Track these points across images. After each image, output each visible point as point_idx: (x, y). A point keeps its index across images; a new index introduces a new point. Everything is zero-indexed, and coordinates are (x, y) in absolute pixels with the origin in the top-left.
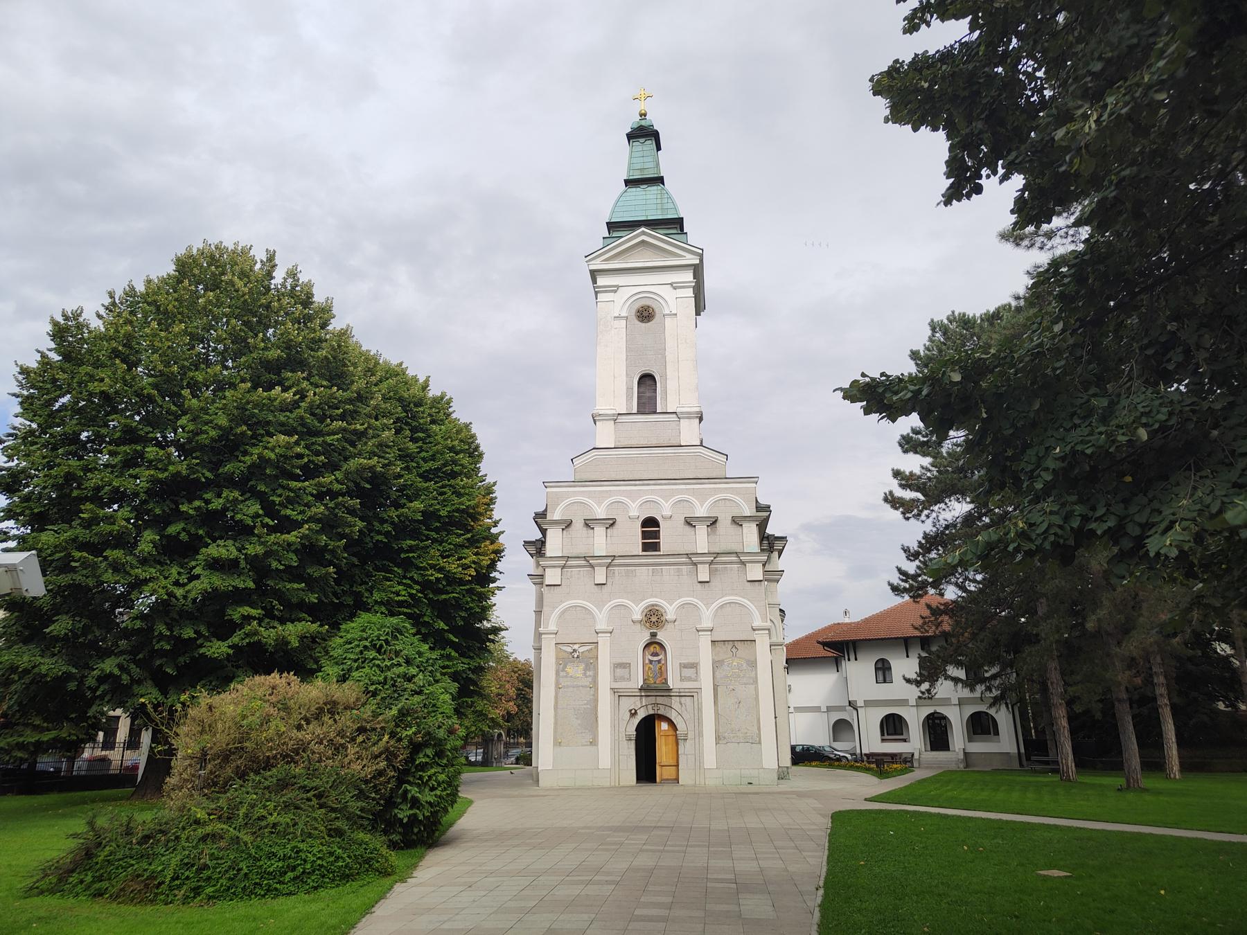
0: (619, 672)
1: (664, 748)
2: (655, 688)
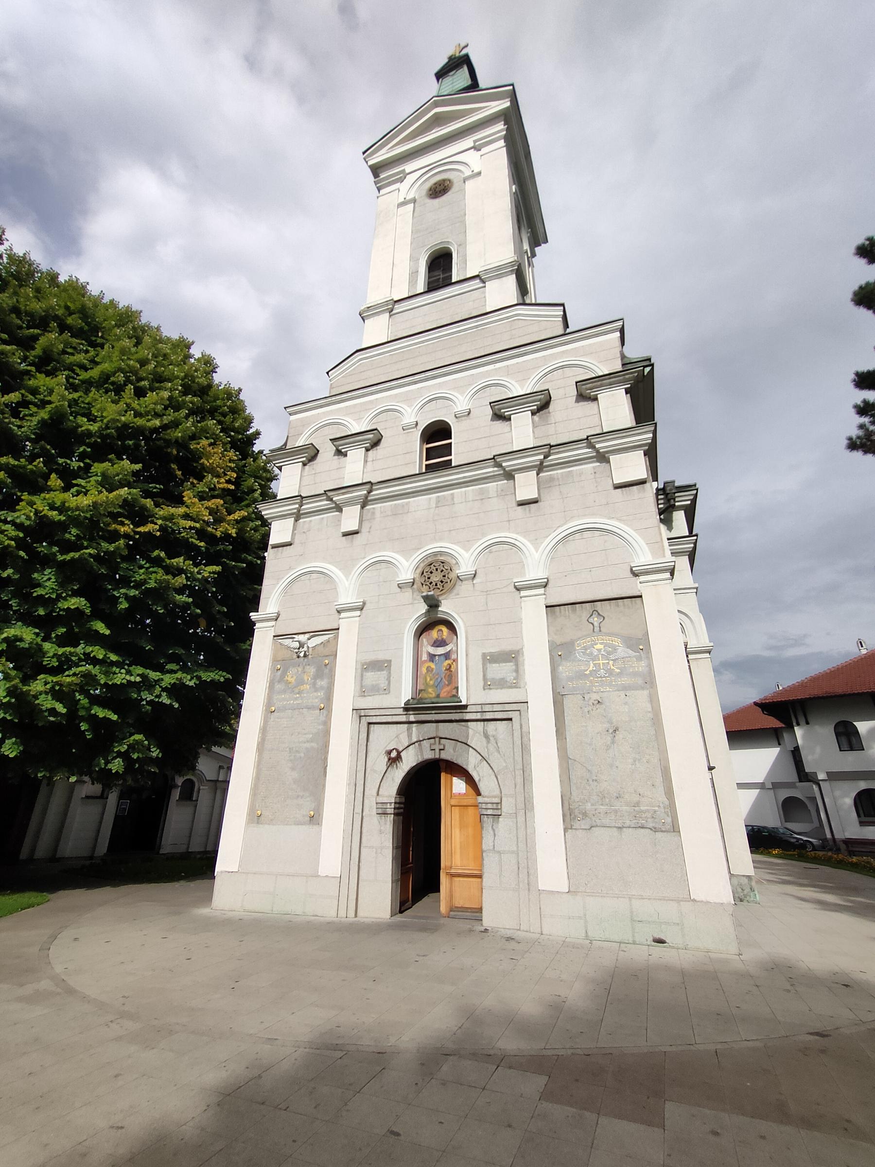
0: (371, 677)
1: (456, 833)
2: (434, 707)
